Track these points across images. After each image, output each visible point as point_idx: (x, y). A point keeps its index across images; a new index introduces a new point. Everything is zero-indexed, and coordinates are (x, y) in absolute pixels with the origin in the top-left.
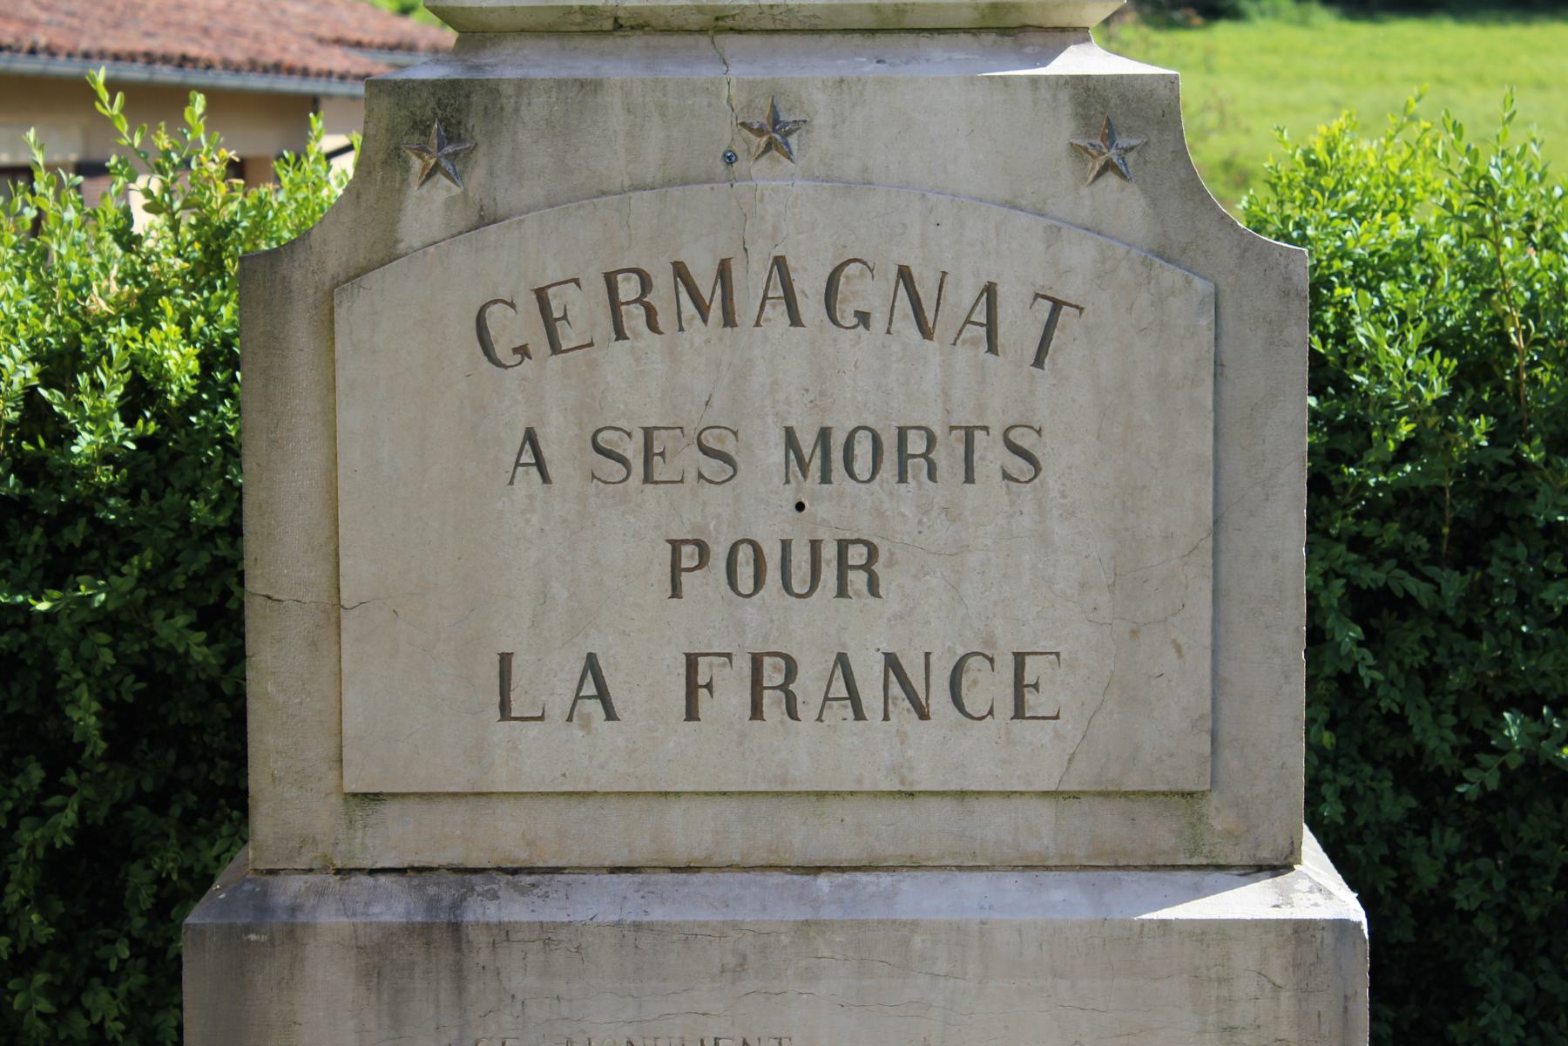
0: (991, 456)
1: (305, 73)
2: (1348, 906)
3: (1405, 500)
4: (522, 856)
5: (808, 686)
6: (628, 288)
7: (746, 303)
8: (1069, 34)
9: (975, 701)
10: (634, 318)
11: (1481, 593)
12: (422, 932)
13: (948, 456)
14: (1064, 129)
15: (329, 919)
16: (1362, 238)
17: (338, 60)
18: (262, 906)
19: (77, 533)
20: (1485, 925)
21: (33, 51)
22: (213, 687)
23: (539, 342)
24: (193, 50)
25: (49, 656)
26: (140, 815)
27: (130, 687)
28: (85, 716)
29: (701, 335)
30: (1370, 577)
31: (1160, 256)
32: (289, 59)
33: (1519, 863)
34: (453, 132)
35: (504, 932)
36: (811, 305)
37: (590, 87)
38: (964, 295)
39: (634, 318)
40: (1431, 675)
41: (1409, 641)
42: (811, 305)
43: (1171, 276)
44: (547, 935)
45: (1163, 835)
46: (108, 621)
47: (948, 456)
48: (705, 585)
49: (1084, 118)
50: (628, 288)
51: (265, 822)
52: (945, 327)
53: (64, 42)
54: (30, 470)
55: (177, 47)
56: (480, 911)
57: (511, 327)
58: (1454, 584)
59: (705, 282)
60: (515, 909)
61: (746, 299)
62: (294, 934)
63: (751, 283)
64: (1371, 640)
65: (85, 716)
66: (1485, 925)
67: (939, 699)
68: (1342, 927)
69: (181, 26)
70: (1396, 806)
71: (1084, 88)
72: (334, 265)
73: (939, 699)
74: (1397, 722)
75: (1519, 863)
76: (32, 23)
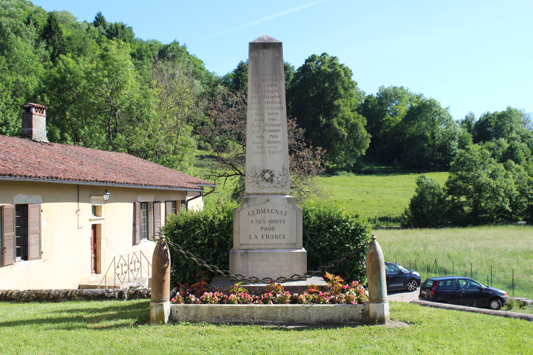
0: (282, 222)
1: (186, 188)
2: (306, 251)
3: (314, 228)
4: (251, 248)
5: (270, 237)
6: (258, 211)
7: (266, 212)
8: (286, 194)
9: (281, 238)
10: (259, 213)
11: (319, 234)
12: (245, 253)
13: (279, 222)
14: (287, 201)
15: (239, 252)
16: (310, 208)
17: (190, 186)
18: (234, 251)
19: (214, 230)
20: (320, 259)
21: (149, 185)
22: (225, 242)
23: (252, 214)
24: (171, 185)
25: (213, 239)
26: (219, 251)
27: (219, 242)
28: (216, 243)
29: (263, 214)
30: (311, 233)
31: (293, 208)
32: (184, 186)
33: (323, 255)
34: (247, 201)
35: (250, 253)
36: (270, 212)
37: (256, 198)
38: (280, 211)
39: (259, 213)
40: (316, 240)
41: (314, 238)
42: (270, 212)
43: (293, 210)
44: (253, 253)
45: (293, 247)
46: (216, 236)
47: (279, 222)
48: (263, 230)
49: (288, 200)
50: (258, 211)
51: (234, 246)
52: (279, 213)
53: (154, 184)
54: (211, 226)
55: (169, 184)
56: (249, 251)
57: (251, 213)
58: (317, 233)
59: (263, 210)
60: (251, 251)
61: (266, 212)
62: (236, 253)
63: (266, 211)
64: (311, 238)
65: (216, 243)
66: (320, 259)
67: (279, 238)
68: (305, 252)
69: (168, 181)
70: (313, 250)
71: (288, 198)
72: (239, 209)
73: (279, 238)
74: (313, 244)
75: (323, 255)
76: (148, 181)
